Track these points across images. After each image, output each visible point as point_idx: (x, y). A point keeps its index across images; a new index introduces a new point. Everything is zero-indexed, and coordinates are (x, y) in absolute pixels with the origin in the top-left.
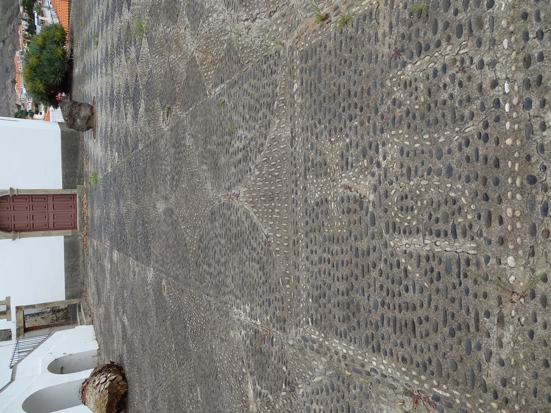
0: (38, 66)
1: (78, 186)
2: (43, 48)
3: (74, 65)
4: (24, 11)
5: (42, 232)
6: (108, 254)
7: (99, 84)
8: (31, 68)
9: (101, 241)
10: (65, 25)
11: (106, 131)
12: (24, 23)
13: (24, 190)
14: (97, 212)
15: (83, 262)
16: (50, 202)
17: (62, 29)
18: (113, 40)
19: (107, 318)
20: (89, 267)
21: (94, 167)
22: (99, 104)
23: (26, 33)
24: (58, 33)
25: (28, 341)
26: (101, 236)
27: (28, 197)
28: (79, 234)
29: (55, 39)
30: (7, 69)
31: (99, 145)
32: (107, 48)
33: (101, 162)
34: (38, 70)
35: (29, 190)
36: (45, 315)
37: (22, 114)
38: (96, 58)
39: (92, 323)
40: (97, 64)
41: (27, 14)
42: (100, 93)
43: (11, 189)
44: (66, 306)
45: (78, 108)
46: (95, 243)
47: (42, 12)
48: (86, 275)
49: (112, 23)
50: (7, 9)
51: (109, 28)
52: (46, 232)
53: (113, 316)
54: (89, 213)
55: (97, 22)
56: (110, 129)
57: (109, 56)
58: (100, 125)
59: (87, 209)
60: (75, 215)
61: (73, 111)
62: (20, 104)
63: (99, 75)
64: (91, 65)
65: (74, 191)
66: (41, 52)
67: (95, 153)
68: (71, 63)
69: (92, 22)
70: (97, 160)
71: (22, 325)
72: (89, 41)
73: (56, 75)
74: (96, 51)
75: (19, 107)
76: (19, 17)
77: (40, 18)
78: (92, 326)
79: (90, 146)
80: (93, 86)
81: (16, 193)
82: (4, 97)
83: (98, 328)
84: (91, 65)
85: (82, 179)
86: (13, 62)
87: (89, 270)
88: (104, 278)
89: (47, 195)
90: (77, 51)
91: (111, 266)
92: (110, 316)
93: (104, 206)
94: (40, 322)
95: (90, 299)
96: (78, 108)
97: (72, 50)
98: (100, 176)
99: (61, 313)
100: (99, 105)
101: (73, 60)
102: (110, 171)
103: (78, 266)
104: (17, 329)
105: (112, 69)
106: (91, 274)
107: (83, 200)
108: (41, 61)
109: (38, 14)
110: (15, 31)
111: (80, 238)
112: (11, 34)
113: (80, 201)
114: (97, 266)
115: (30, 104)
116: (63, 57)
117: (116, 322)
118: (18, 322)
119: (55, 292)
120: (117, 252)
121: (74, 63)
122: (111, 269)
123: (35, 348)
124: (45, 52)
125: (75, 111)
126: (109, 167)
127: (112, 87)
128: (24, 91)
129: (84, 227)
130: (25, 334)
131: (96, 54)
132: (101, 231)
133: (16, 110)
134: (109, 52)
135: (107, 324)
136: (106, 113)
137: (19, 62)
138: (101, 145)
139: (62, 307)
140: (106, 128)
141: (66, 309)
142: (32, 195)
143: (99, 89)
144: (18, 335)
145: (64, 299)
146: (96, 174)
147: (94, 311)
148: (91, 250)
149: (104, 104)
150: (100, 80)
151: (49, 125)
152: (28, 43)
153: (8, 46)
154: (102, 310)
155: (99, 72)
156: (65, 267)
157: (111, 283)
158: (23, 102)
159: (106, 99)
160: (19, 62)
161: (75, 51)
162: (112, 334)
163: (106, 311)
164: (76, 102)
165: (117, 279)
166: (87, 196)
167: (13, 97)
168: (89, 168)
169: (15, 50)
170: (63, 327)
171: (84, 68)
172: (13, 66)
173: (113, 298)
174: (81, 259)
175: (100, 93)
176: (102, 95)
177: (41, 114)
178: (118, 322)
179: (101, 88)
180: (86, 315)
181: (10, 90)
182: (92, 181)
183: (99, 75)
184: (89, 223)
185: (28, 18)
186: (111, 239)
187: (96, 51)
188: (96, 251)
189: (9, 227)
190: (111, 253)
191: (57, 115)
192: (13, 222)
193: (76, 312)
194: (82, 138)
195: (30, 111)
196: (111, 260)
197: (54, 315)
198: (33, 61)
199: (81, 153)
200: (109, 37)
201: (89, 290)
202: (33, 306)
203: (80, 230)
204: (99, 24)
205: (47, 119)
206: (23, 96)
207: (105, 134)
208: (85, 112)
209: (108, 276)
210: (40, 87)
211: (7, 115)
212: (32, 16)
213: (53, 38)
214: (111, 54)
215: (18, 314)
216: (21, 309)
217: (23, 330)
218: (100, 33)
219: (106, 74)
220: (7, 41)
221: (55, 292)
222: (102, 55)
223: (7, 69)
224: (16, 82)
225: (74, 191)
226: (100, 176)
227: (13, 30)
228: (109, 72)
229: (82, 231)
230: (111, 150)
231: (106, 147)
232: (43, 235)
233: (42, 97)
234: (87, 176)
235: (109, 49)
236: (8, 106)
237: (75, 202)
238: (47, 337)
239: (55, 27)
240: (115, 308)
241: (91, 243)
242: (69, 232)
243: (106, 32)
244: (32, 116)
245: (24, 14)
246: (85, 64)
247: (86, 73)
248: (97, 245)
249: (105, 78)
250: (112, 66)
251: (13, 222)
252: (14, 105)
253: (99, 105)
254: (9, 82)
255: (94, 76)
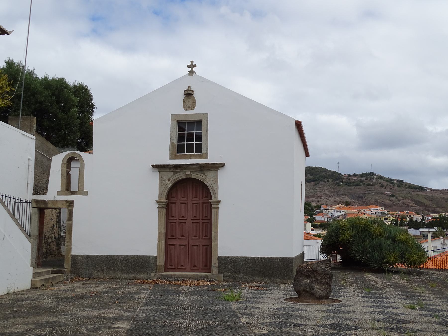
0: (371, 235)
1: (222, 275)
2: (394, 240)
3: (379, 275)
4: (433, 218)
5: (164, 232)
6: (126, 314)
7: (359, 308)
8: (367, 226)
9: (145, 304)
10: (426, 265)
11: (297, 316)
12: (420, 217)
13: (217, 215)
14: (186, 299)
15: (120, 278)
16: (200, 242)
17: (422, 262)
18: (421, 331)
19: (36, 310)
20: (111, 286)
21: (247, 298)
22: (332, 308)
23: (408, 219)
24: (415, 258)
25: (27, 214)
26: (152, 304)
27: (208, 218)
28: (158, 274)
29: (408, 255)
30: (362, 197)
31: (277, 306)
32: (409, 322)
33: (254, 308)
34: (366, 234)
35: (217, 220)
36: (56, 230)
37: (310, 211)
38: (393, 305)
39: (33, 287)
40: (385, 307)
41: (430, 221)
42: (347, 309)
43: (219, 202)
44: (63, 254)
45: (323, 281)
46: (144, 295)
47: (437, 237)
48: (100, 281)
49: (444, 331)
50: (431, 201)
51: (436, 326)
52: (163, 236)
53: (36, 319)
54: (186, 287)
55: (440, 308)
56: (299, 322)
57: (398, 325)
58: (304, 307)
59: (191, 285)
60: (184, 270)
61: (320, 275)
62: (322, 208)
63: (371, 310)
64: (382, 298)
65: (215, 270)
66: (388, 238)
67: (265, 300)
68: (379, 271)
69: (438, 301)
70: (256, 302)
71: (50, 206)
72: (413, 297)
73: (363, 254)
74: (401, 306)
75: (319, 207)
76: (425, 212)
77: (430, 235)
78: (28, 287)
79: (275, 292)
80: (354, 299)
81: (214, 206)
82: (328, 193)
83: (24, 296)
84: (382, 298)
85: (231, 280)
86: (371, 204)
87: (107, 286)
88: (93, 308)
89: (210, 239)
90: (397, 279)
91: (109, 319)
92: (37, 314)
93: (193, 311)
94: (49, 224)
95: (68, 286)
96: (323, 281)
97: (397, 272)
98: (234, 306)
99: (55, 248)
100: (330, 308)
101: (385, 273)
102: (242, 320)
103: (115, 271)
104: (45, 201)
105: (381, 328)
106: (101, 288)
107: (203, 280)
108: (377, 237)
109: (434, 233)
110: (408, 207)
111: (152, 275)
112: (403, 203)
113: (201, 277)
114: (111, 298)
115: (323, 219)
116: (387, 262)
117: (27, 324)
118: (53, 202)
119: (85, 241)
120: (128, 327)
121: (382, 275)
122: (104, 318)
123: (17, 221)
124: (389, 242)
125: (319, 278)
126: (247, 320)
127: (357, 328)
128: (337, 214)
129: (167, 280)
130: (36, 209)
131: (399, 306)
132: (159, 304)
133: (314, 204)
134: (404, 325)
135: (27, 309)
136: (321, 318)
137: (372, 210)
138: (278, 309)
139: (63, 249)
140: (301, 317)
141: (60, 253)
142: (211, 223)
143: (351, 309)
144: (37, 201)
145: (73, 253)
146: (237, 300)
147: (49, 292)
148: (134, 289)
149: (333, 315)
150: (365, 310)
151: (299, 243)
152: (396, 221)
153: (389, 200)
154: (48, 302)
155: (375, 310)
156: (115, 256)
157: (84, 318)
158: (324, 212)
159: (339, 317)
160: (372, 210)
161: (397, 276)
162: (10, 318)
163: (46, 308)
164: (331, 279)
165: (90, 327)
166: (208, 286)
167: (329, 202)
168: (245, 291)
169: (385, 206)
170: (35, 250)
171: (377, 288)
172: (366, 204)
173: (63, 320)
174: (124, 276)
175: (347, 309)
176: (344, 312)
177: (312, 230)
178: (25, 327)
179: (353, 312)
180: (47, 280)
181: (337, 199)
182: (228, 294)
183: (371, 310)
184: (172, 288)
185: (426, 221)
186: (147, 319)
187: (401, 306)
188: (132, 296)
189: (174, 197)
190: (127, 319)
191: (313, 252)
192: (178, 221)
193: (53, 266)
194: (284, 281)
195: (315, 219)
196: (116, 319)
197: (54, 239)
198: (377, 229)
199: (266, 280)
200: (424, 326)
201: (79, 284)
202: (70, 218)
203: (163, 275)
204: (438, 311)
205: (307, 237)
206: (331, 212)
207: (292, 315)
208: (319, 289)
209: (96, 313)
210: (346, 235)
211: (307, 195)
212: (430, 225)
213: (409, 252)
214: (401, 327)
215: (65, 202)
216: (69, 206)
217: (43, 206)
218: (426, 313)
219: (373, 320)
220: (393, 199)
221: (85, 241)
222: (398, 314)
223: (362, 197)
224: (347, 205)
225: (215, 270)
226: (234, 306)
227: (408, 206)
228: (377, 325)
229: (162, 277)
230: (271, 324)
231: (274, 316)
232: (159, 233)
233: (333, 236)
234: (235, 287)
235: (408, 325)
236: (317, 196)
237: (200, 270)
238: (26, 234)
239: (423, 254)
240: (48, 323)
241: (144, 289)
242: (161, 262)
243: (430, 322)
244: (308, 220)
245: (430, 218)
246: (382, 289)
247: (370, 291)
248: (140, 298)
249: (367, 317)
250: (386, 328)
251: (178, 202)
252: (320, 203)
253: (330, 308)
254: (347, 199)
255: (368, 302)
